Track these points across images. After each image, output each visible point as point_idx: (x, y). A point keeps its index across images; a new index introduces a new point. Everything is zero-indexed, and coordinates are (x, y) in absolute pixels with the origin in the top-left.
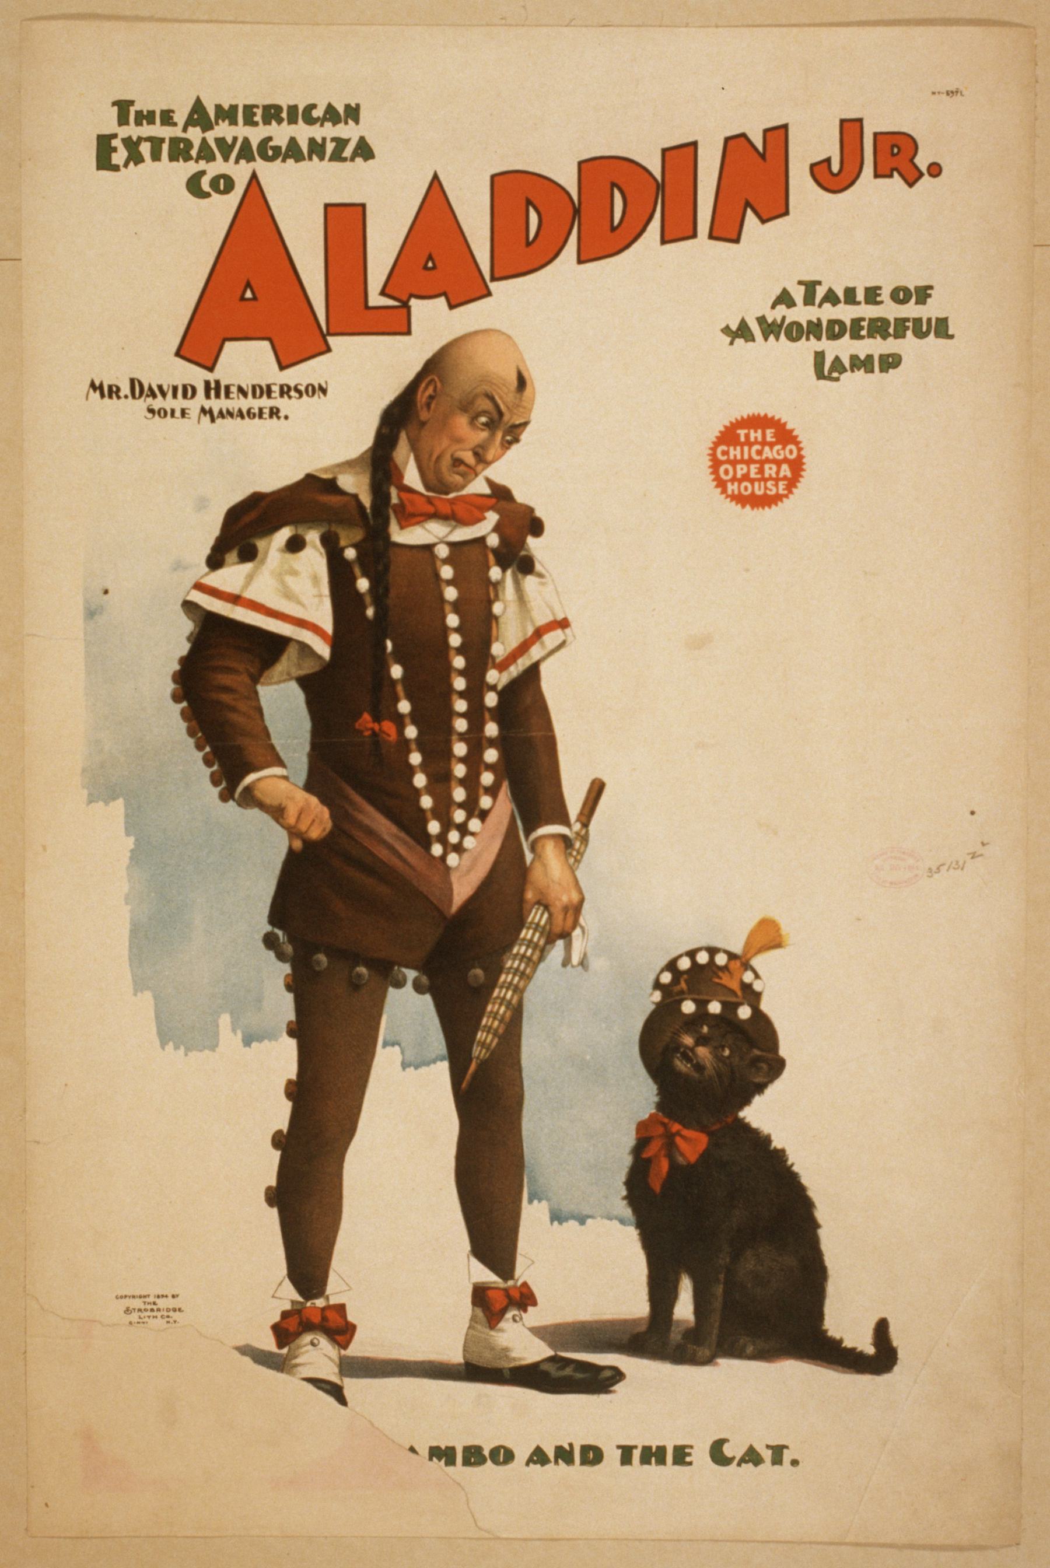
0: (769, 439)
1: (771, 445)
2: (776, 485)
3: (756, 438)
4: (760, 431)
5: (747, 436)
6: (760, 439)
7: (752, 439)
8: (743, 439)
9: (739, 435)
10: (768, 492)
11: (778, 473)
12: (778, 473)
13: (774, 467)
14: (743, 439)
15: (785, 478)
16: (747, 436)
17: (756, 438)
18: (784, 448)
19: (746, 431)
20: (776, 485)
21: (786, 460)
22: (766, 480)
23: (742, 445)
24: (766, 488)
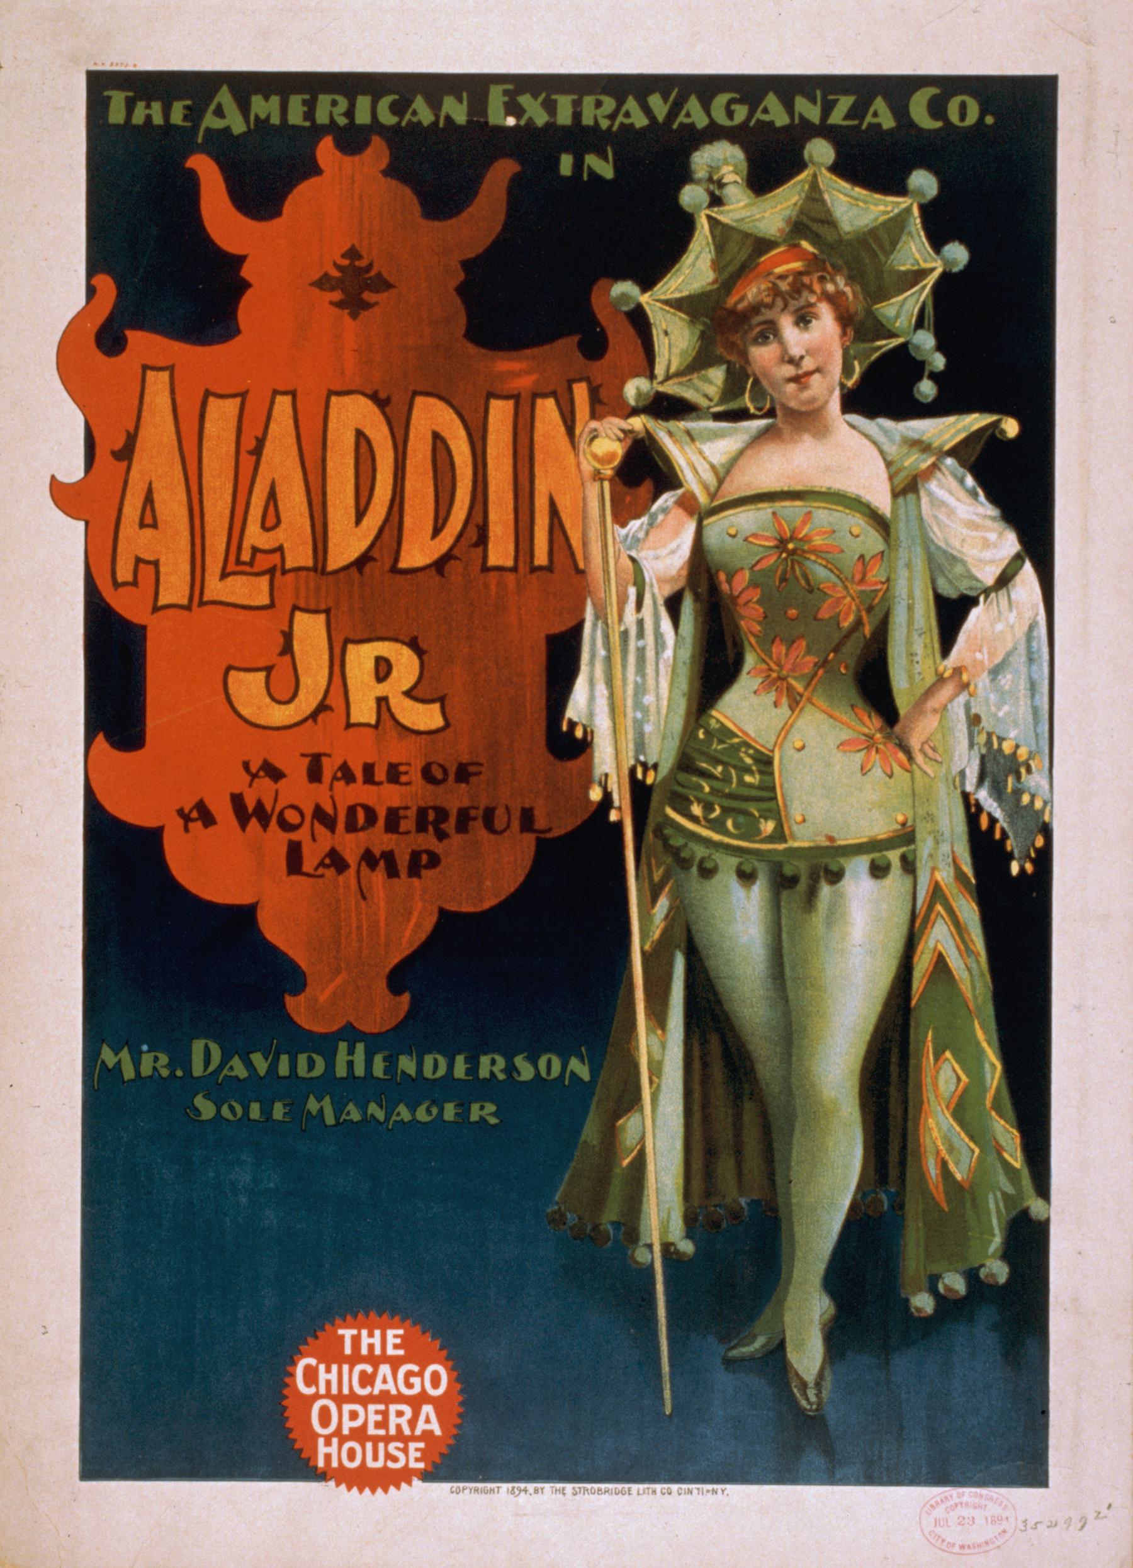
0: (390, 1351)
1: (395, 1363)
2: (405, 1451)
3: (371, 1347)
4: (377, 1333)
5: (356, 1340)
6: (378, 1351)
7: (364, 1351)
8: (348, 1351)
9: (343, 1337)
10: (390, 1464)
11: (413, 1423)
12: (413, 1423)
13: (407, 1410)
14: (348, 1351)
15: (427, 1435)
16: (356, 1340)
17: (371, 1347)
18: (420, 1374)
19: (355, 1332)
20: (405, 1451)
21: (423, 1398)
22: (387, 1439)
23: (341, 1359)
24: (389, 1457)
